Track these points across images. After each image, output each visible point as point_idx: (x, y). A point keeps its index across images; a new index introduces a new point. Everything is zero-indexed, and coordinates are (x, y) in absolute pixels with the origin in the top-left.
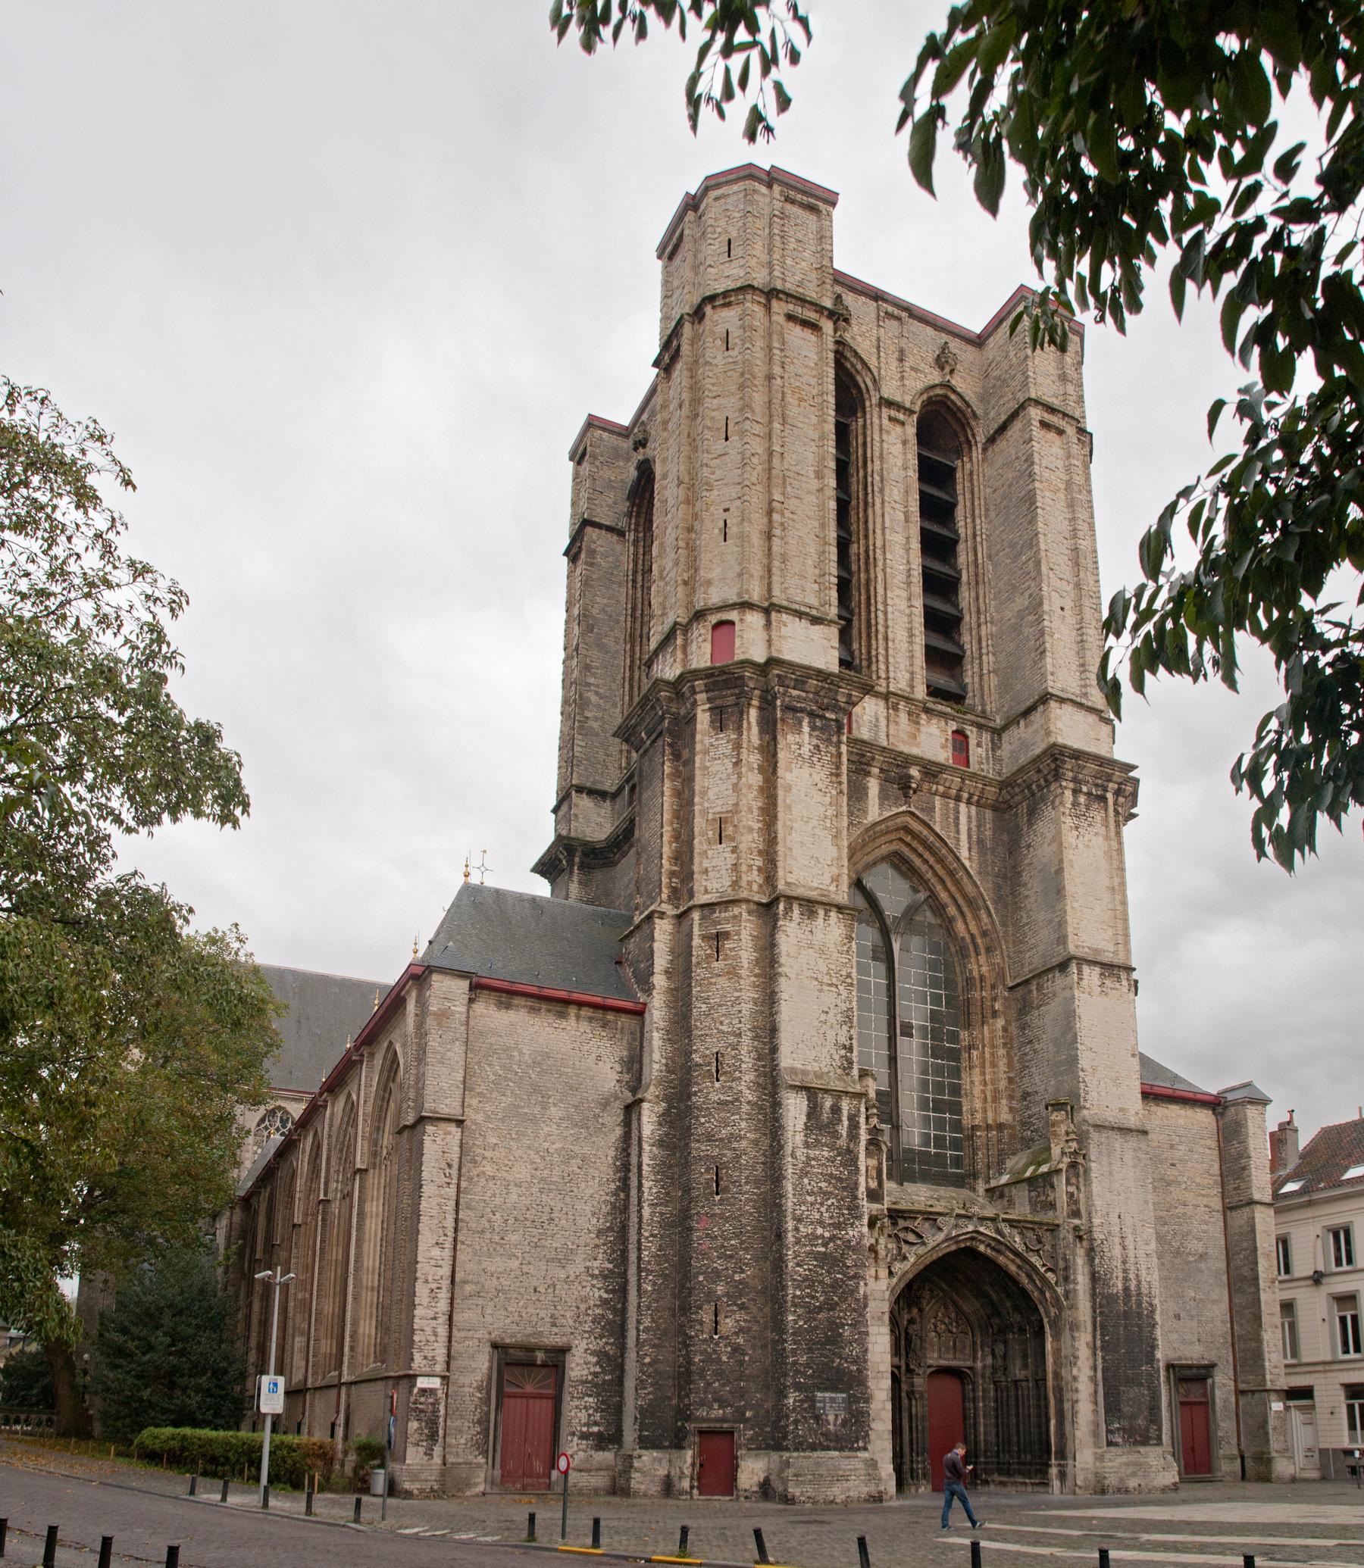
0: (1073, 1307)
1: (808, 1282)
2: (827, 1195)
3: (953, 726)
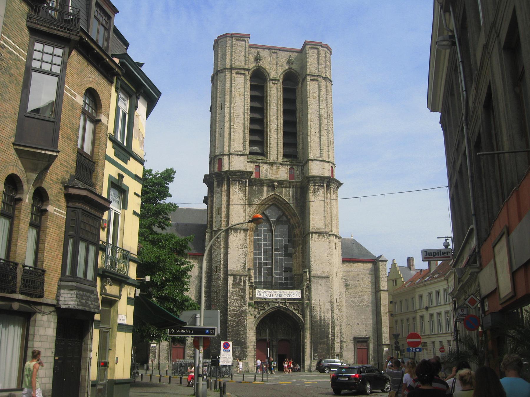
0: (306, 324)
3: (289, 167)
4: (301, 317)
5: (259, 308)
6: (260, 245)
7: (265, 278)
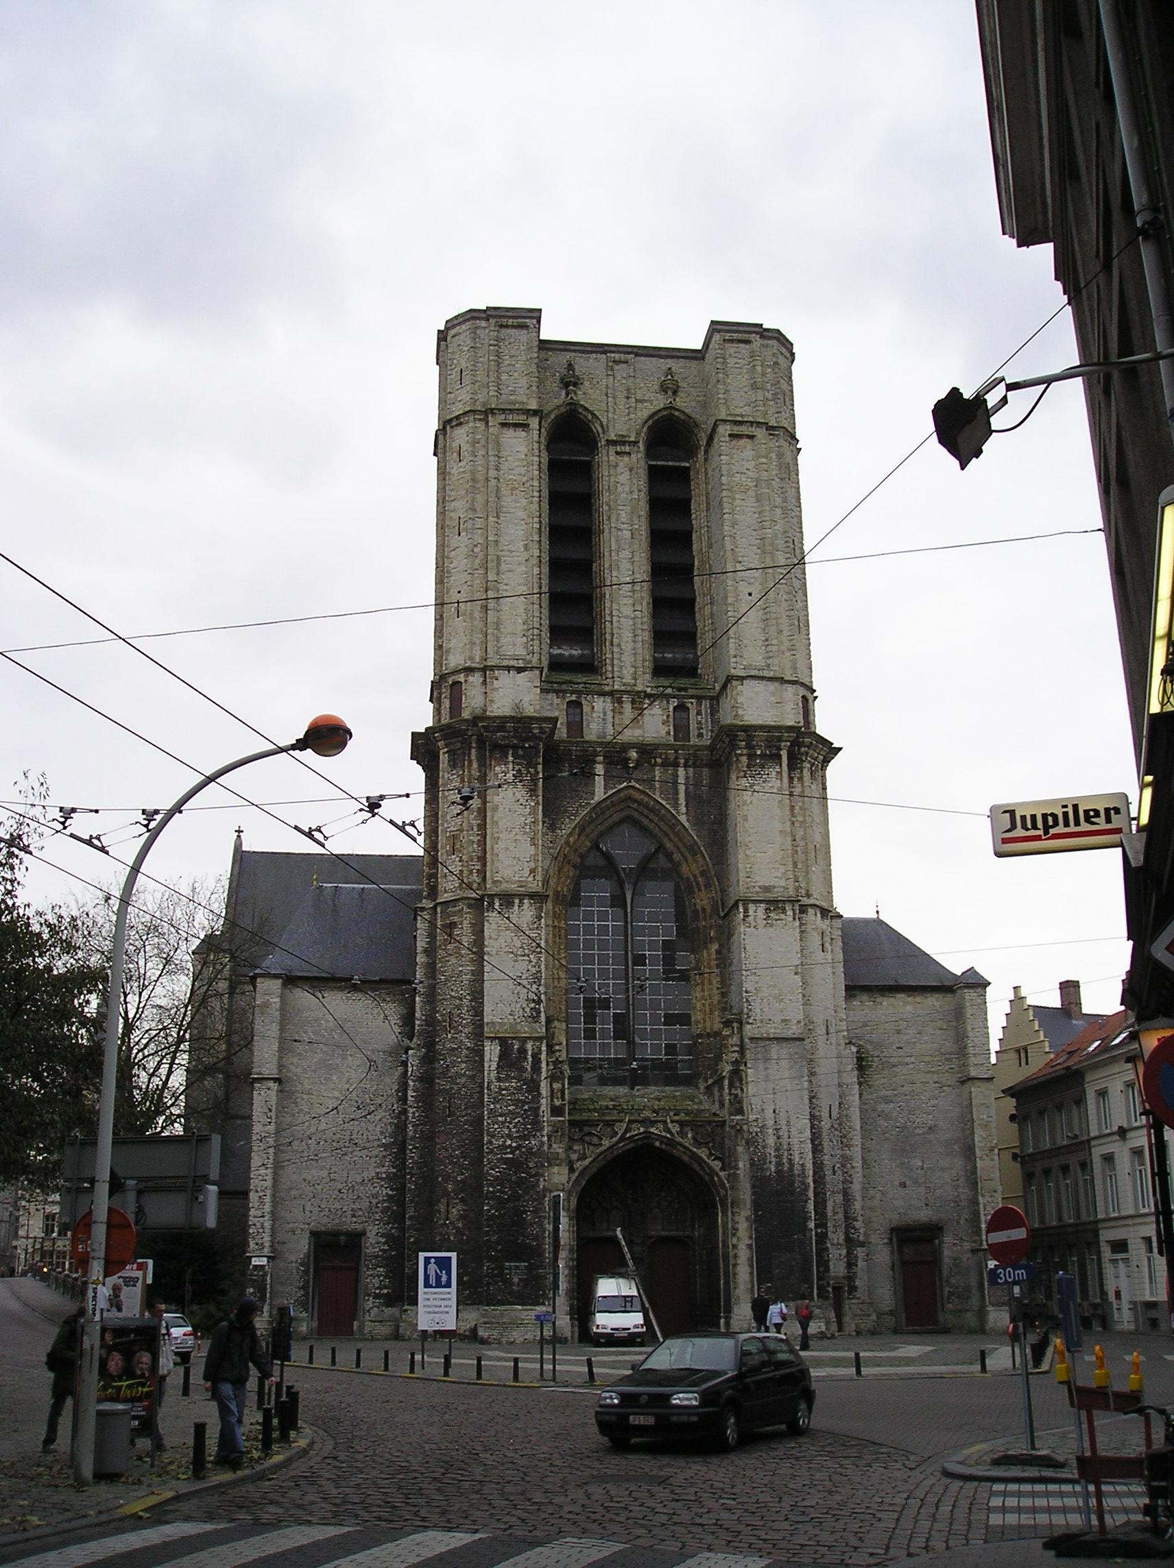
1: (500, 1180)
3: (674, 702)
4: (716, 1165)
5: (587, 1138)
7: (604, 1047)
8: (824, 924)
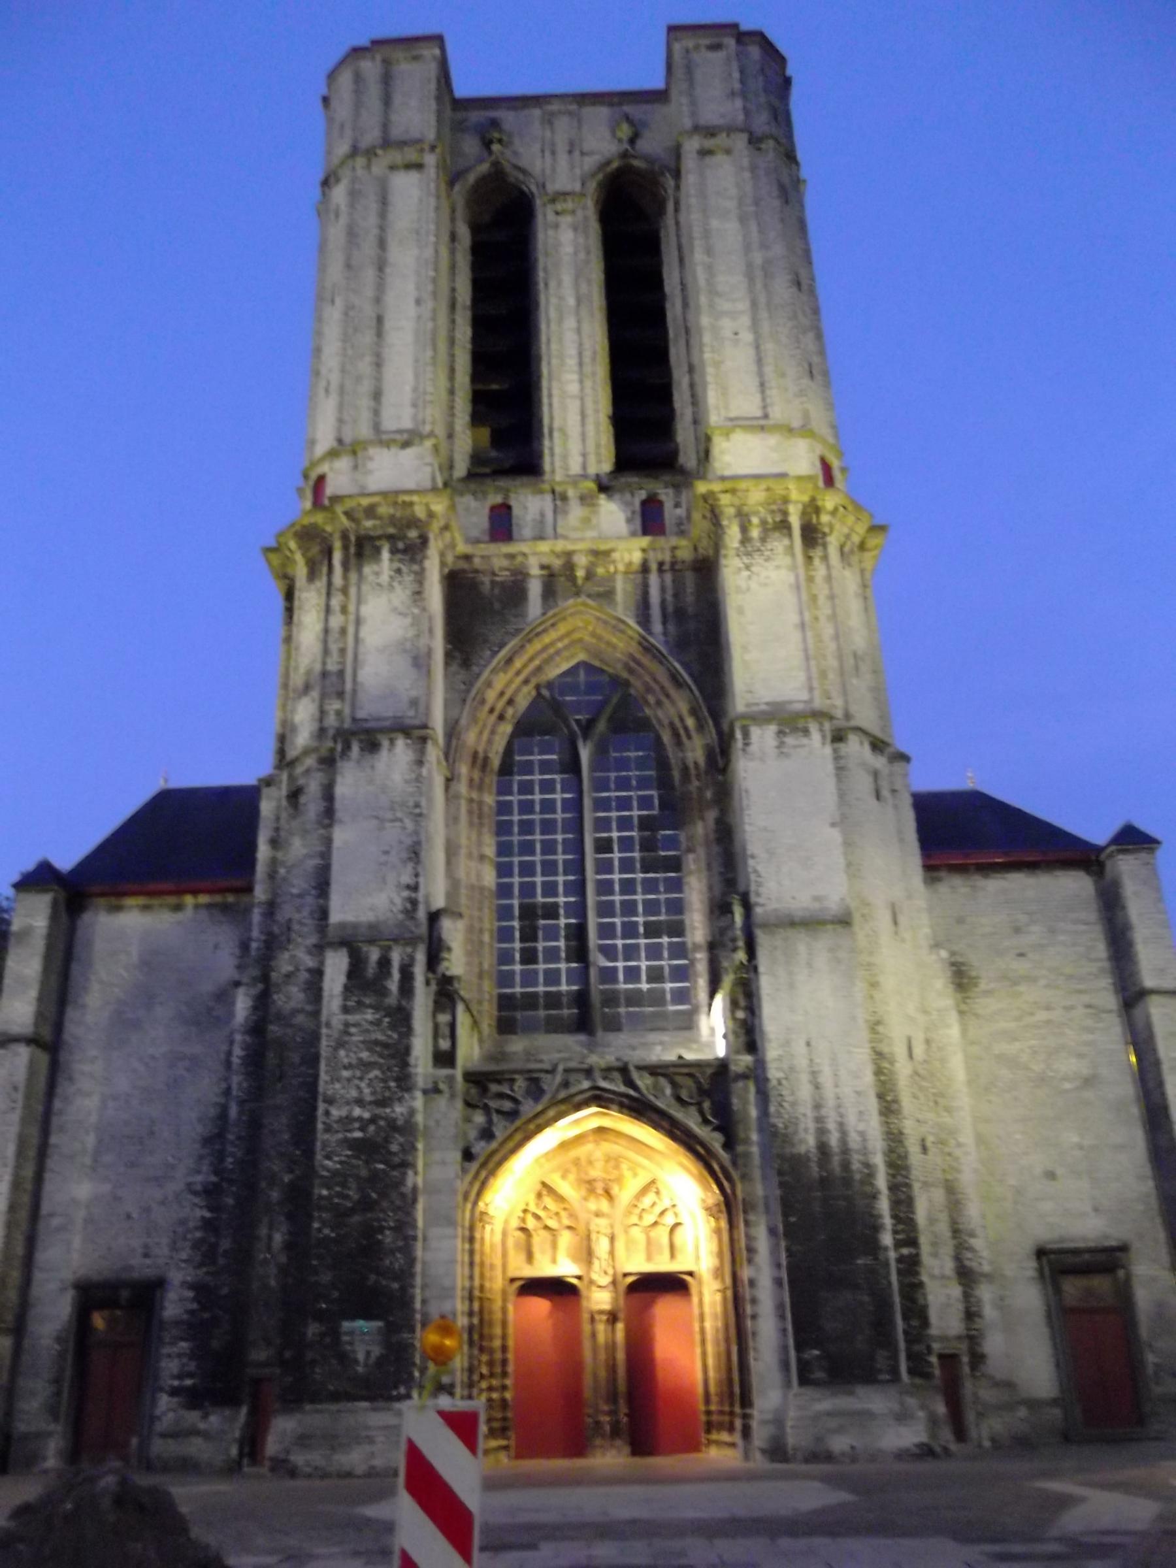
1: (339, 1178)
2: (367, 1066)
3: (643, 495)
5: (493, 1104)
6: (526, 827)
8: (880, 762)
